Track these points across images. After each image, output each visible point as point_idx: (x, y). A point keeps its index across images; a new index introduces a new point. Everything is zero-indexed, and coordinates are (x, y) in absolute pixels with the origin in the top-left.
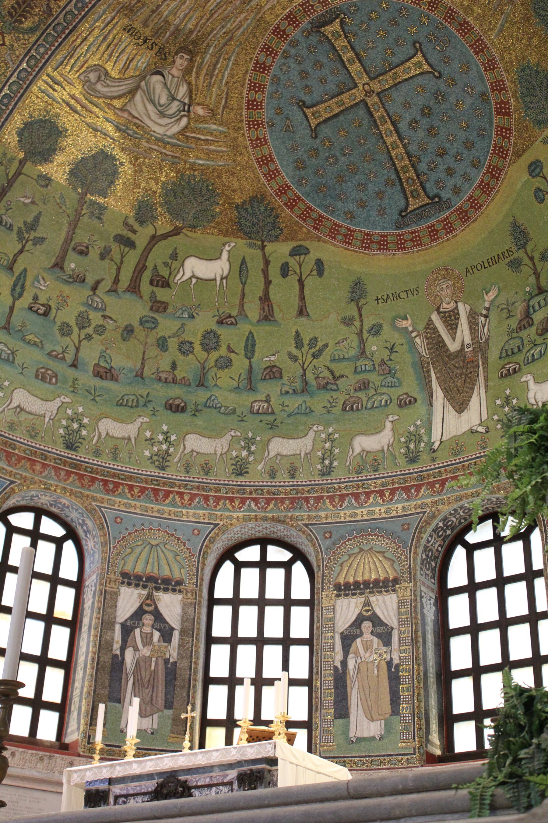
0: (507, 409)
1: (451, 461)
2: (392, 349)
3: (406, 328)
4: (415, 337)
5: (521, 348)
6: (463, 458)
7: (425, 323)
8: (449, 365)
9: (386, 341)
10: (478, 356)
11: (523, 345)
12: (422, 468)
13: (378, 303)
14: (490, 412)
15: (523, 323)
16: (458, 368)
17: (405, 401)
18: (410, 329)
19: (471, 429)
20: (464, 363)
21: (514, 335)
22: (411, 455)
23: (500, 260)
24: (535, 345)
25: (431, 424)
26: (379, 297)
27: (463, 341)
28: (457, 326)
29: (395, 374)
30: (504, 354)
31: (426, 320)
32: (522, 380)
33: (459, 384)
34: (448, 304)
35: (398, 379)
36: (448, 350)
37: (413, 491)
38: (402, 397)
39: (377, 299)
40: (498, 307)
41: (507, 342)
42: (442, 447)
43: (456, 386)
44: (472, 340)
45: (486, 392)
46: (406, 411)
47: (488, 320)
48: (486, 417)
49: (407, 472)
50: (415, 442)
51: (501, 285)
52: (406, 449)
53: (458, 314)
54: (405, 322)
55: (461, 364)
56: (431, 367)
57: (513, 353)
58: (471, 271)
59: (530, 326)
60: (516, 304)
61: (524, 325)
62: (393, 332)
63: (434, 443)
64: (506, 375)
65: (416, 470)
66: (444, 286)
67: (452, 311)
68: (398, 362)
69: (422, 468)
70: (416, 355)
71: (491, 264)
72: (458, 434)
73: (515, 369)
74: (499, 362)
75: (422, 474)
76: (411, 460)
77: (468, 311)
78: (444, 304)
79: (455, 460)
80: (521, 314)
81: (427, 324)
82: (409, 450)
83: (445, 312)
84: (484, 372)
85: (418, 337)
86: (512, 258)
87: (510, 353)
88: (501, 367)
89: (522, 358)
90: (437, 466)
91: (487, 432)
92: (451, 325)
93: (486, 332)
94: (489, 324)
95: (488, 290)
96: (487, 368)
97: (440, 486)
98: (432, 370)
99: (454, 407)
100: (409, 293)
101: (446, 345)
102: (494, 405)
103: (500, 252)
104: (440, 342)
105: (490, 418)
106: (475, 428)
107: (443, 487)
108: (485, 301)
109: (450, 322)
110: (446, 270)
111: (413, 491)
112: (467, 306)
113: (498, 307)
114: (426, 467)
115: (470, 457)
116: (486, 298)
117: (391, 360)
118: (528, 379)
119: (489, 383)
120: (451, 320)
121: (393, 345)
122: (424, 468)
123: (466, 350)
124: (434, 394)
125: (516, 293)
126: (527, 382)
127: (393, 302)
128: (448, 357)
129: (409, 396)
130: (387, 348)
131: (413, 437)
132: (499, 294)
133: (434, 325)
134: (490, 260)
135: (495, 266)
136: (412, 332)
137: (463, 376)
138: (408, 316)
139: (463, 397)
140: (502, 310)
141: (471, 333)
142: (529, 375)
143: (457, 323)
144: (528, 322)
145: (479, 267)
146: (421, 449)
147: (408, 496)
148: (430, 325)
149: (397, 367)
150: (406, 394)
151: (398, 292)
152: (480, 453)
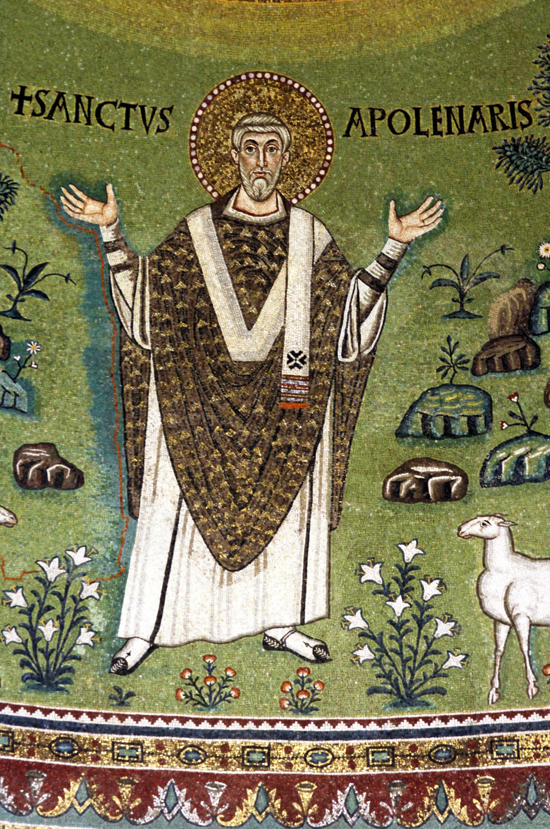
0: (399, 605)
1: (183, 720)
2: (26, 282)
3: (95, 229)
4: (119, 268)
5: (481, 429)
6: (228, 722)
7: (162, 235)
8: (214, 399)
9: (14, 248)
10: (323, 403)
11: (489, 419)
12: (77, 714)
13: (20, 111)
14: (338, 597)
15: (501, 350)
16: (244, 420)
17: (42, 472)
18: (107, 236)
19: (263, 632)
20: (268, 408)
21: (463, 378)
22: (42, 661)
23: (478, 128)
24: (531, 433)
25: (123, 574)
26: (31, 91)
27: (281, 337)
28: (270, 285)
29: (21, 366)
30: (416, 427)
31: (170, 226)
32: (467, 529)
33: (239, 474)
34: (258, 199)
35: (28, 386)
36: (222, 348)
37: (36, 785)
38: (31, 453)
39: (21, 97)
40: (428, 270)
41: (433, 390)
42: (153, 663)
43: (229, 475)
44: (312, 344)
45: (331, 528)
46: (38, 503)
47: (381, 300)
48: (322, 611)
49: (23, 713)
50: (61, 618)
51: (457, 206)
52: (27, 635)
53: (285, 244)
54: (93, 206)
55: (260, 409)
56: (153, 387)
57: (448, 433)
58: (368, 127)
59: (524, 366)
60: (492, 283)
61: (504, 359)
62: (44, 225)
63: (127, 640)
64: (410, 493)
65: (53, 717)
66: (262, 139)
67: (269, 227)
68: (39, 331)
69: (77, 714)
70: (109, 328)
71: (443, 127)
72: (216, 638)
73: (447, 485)
74: (393, 444)
75: (75, 734)
76: (40, 678)
77: (321, 246)
78: (243, 194)
79: (198, 722)
80: (502, 319)
81: (169, 241)
82: (35, 641)
83: (239, 224)
84: (334, 461)
85: (128, 273)
86: (520, 134)
87: (437, 430)
88: (395, 464)
89: (479, 461)
90: (129, 722)
91: (319, 660)
92: (250, 271)
93: (365, 337)
94: (383, 315)
95: (407, 204)
96: (347, 450)
97: (134, 795)
98: (153, 396)
99: (210, 543)
100: (136, 114)
101: (217, 331)
102: (353, 580)
103: (485, 103)
104: (198, 314)
105: (336, 615)
106: (278, 634)
107: (148, 802)
108: (386, 236)
109: (248, 261)
110: (286, 89)
111: (36, 785)
112: (320, 229)
113: (428, 270)
114: (92, 715)
115: (251, 726)
116: (394, 227)
117: (16, 315)
118: (488, 531)
119: (345, 504)
120: (255, 258)
121: (36, 270)
122: (85, 719)
123: (286, 370)
124: (147, 479)
125: (503, 249)
126: (485, 539)
127: (72, 126)
128: (217, 372)
129: (56, 456)
130: (12, 270)
131: (52, 601)
132: (441, 229)
133: (192, 251)
134: (443, 115)
135: (454, 138)
136: (110, 248)
137: (257, 451)
138: (110, 189)
139: (248, 519)
140: (439, 283)
141: (313, 323)
142: (493, 521)
143: (274, 274)
144: (521, 353)
145: (399, 122)
146: (80, 651)
147: (19, 801)
148: (177, 247)
149: (33, 348)
150: (49, 446)
151: (98, 100)
152: (288, 723)
